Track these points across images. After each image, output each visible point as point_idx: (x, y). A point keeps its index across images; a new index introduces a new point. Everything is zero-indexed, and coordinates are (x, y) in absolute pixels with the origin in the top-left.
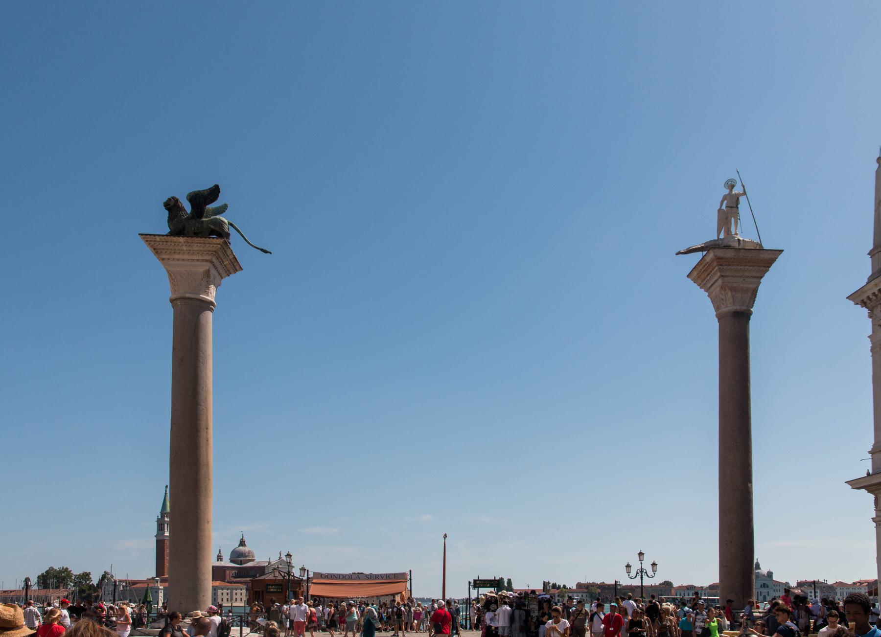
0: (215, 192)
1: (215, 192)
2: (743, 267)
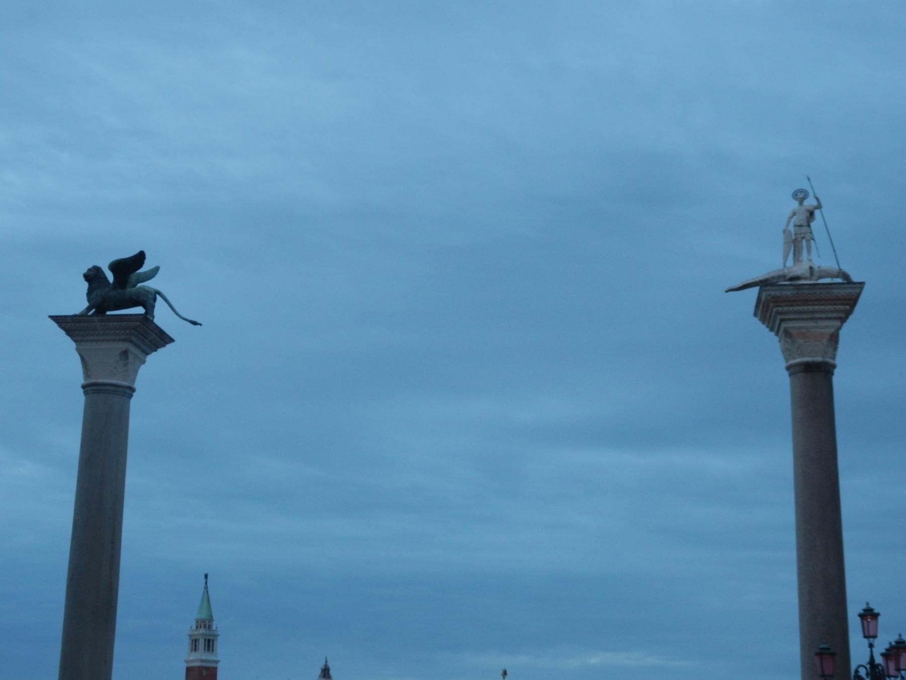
0: (140, 258)
1: (140, 258)
2: (811, 308)
